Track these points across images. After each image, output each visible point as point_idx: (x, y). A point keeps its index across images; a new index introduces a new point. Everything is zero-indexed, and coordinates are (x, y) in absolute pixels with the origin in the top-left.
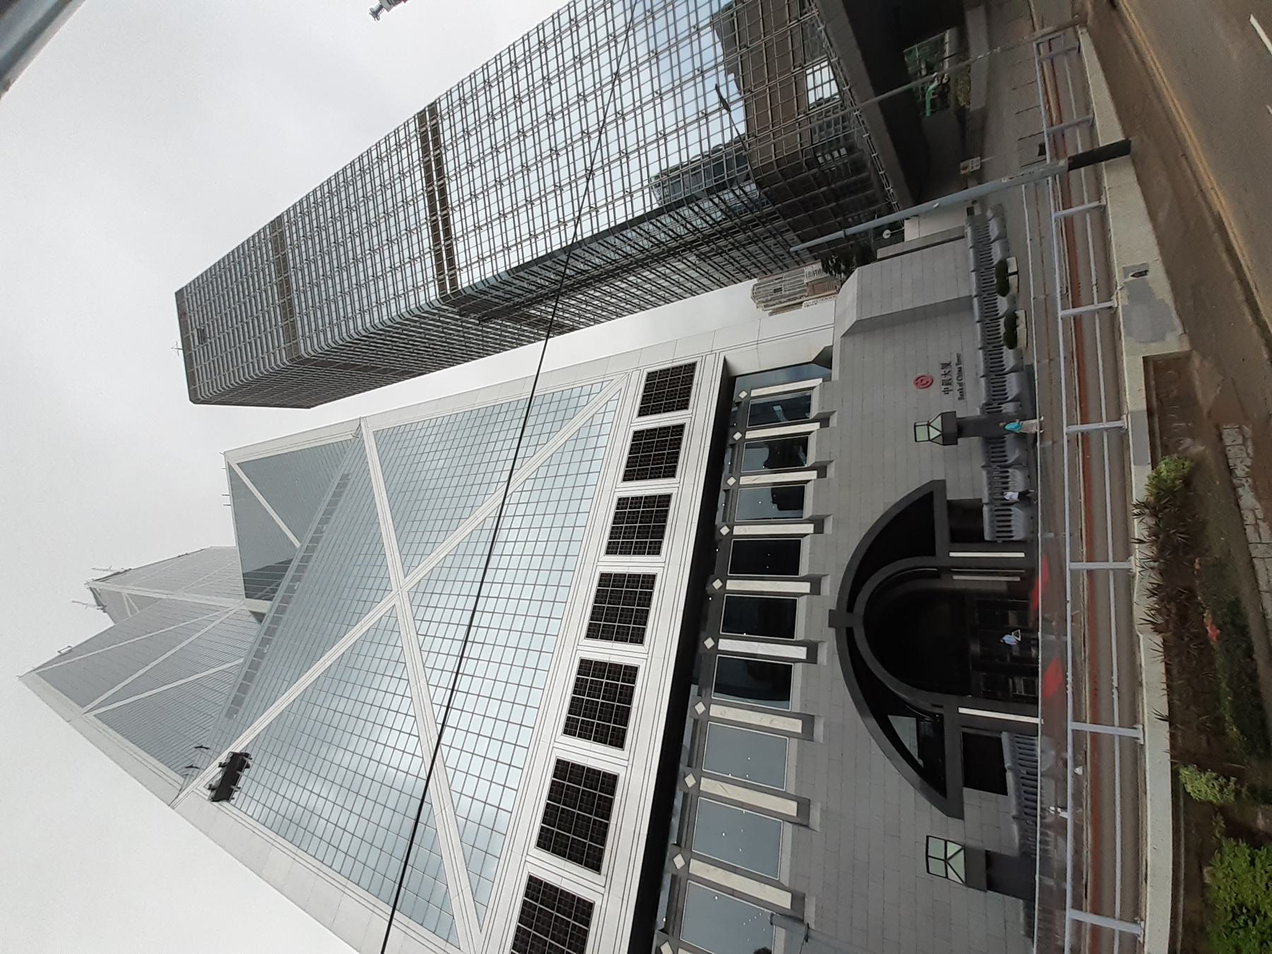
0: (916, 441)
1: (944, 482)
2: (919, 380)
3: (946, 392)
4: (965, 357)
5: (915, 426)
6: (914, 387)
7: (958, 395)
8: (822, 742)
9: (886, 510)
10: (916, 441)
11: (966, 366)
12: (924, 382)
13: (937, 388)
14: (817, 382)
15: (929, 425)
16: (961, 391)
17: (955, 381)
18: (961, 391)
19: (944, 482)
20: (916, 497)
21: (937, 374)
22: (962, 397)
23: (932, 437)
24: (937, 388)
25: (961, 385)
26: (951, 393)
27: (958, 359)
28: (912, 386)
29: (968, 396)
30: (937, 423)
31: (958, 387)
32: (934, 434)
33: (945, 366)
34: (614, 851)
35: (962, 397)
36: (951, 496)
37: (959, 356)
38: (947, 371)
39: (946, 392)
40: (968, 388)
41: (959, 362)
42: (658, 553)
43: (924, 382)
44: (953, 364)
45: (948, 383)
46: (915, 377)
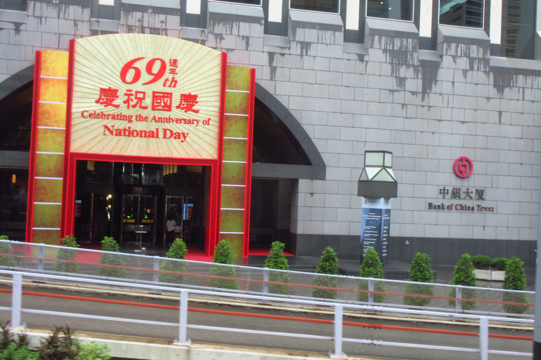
0: (366, 152)
1: (323, 178)
2: (466, 162)
3: (443, 192)
4: (489, 216)
5: (384, 152)
7: (436, 203)
9: (293, 113)
10: (366, 152)
11: (476, 217)
12: (463, 168)
13: (452, 182)
15: (384, 167)
16: (440, 207)
17: (455, 202)
18: (440, 207)
19: (323, 178)
20: (304, 145)
23: (367, 169)
24: (452, 182)
25: (450, 208)
26: (441, 196)
27: (486, 209)
28: (458, 154)
29: (433, 213)
30: (384, 177)
31: (447, 203)
32: (371, 173)
33: (480, 194)
35: (430, 205)
36: (303, 185)
37: (491, 209)
38: (473, 195)
39: (443, 192)
40: (442, 215)
41: (481, 209)
43: (463, 168)
44: (480, 202)
45: (456, 194)
46: (471, 158)
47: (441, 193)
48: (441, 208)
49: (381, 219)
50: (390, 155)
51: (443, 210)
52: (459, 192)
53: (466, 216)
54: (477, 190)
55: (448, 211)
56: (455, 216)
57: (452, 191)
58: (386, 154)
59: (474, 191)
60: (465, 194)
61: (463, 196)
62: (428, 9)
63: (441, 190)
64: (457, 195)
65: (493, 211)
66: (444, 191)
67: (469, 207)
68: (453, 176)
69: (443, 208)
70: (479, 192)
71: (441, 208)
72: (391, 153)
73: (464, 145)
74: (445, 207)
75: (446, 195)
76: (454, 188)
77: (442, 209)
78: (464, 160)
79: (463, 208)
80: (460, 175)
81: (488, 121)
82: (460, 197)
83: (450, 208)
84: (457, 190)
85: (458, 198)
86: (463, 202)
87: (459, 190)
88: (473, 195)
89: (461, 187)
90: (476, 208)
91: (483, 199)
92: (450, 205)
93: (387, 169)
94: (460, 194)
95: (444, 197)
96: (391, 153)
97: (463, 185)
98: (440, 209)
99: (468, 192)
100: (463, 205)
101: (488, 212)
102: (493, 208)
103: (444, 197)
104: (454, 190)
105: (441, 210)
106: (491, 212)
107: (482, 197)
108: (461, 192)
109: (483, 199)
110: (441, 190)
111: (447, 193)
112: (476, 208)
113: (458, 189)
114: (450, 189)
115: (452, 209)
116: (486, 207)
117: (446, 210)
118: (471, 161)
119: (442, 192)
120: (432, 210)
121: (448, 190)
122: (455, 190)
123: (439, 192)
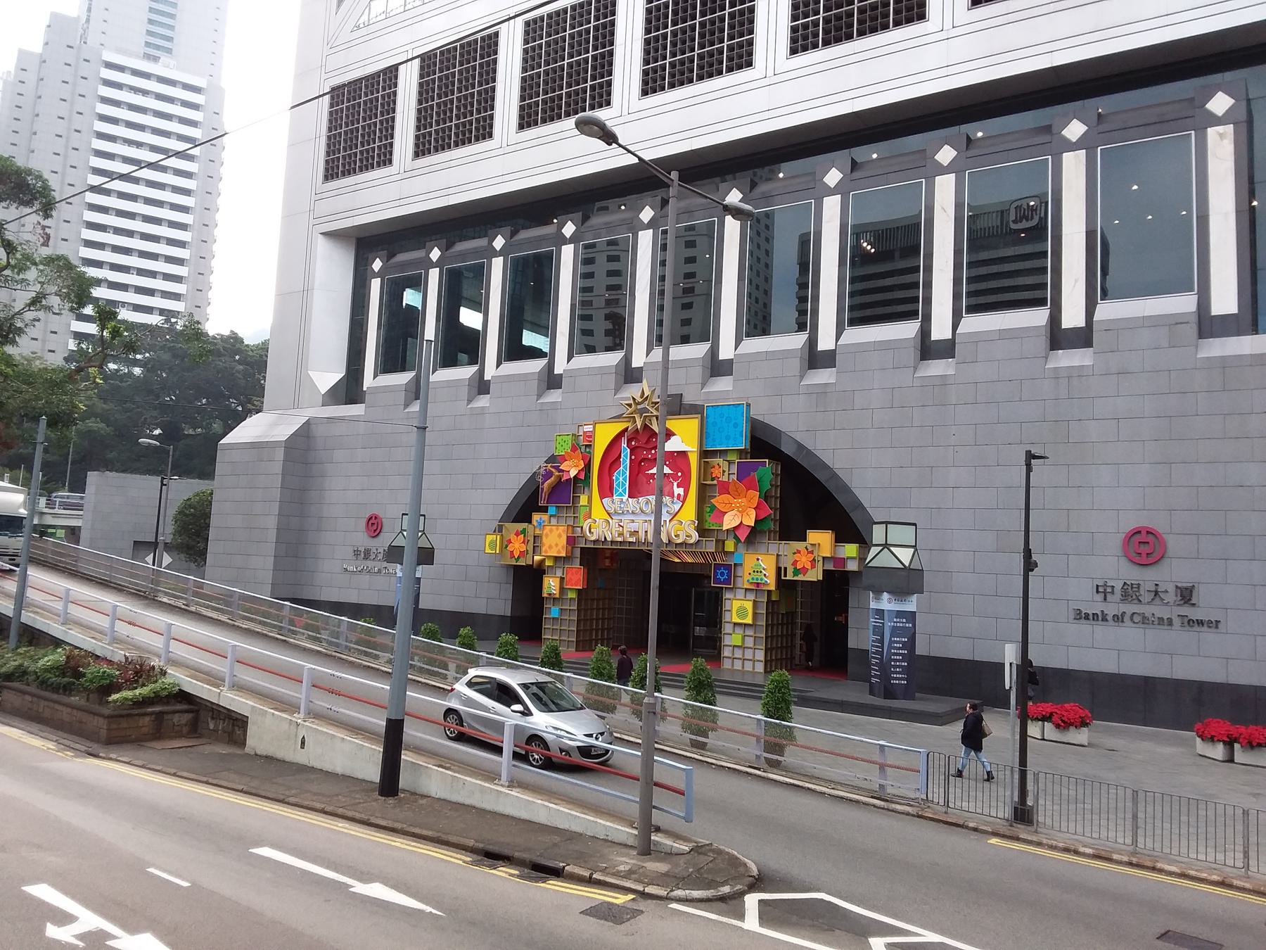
4: (1208, 635)
5: (887, 523)
6: (1133, 525)
8: (1198, 356)
9: (840, 473)
11: (1178, 637)
14: (1225, 300)
17: (1129, 608)
21: (1170, 574)
22: (1081, 616)
24: (1119, 571)
25: (1119, 619)
26: (1100, 597)
27: (1201, 623)
28: (1131, 522)
29: (1085, 627)
31: (1111, 609)
33: (1186, 595)
34: (432, 168)
39: (1103, 591)
40: (1101, 631)
42: (750, 64)
44: (1186, 611)
45: (1130, 592)
47: (1098, 592)
48: (1100, 619)
49: (883, 623)
50: (914, 527)
51: (1105, 623)
52: (1138, 591)
53: (1154, 636)
54: (1177, 587)
55: (1117, 624)
56: (1130, 634)
57: (1122, 588)
58: (888, 525)
59: (1171, 589)
60: (1153, 594)
61: (1146, 597)
62: (1076, 281)
63: (1097, 586)
64: (1134, 597)
65: (1217, 627)
66: (1105, 590)
67: (1161, 619)
68: (1124, 561)
69: (1104, 619)
70: (1181, 591)
71: (1100, 619)
72: (915, 524)
73: (1144, 506)
74: (1109, 618)
75: (1109, 596)
76: (1125, 583)
77: (1102, 620)
78: (1144, 533)
79: (1145, 620)
80: (1145, 560)
81: (1197, 460)
82: (1140, 601)
83: (1119, 619)
84: (1132, 588)
85: (1136, 601)
86: (1147, 610)
87: (1139, 588)
88: (1171, 597)
89: (1140, 582)
90: (1177, 621)
91: (1194, 605)
92: (1120, 614)
93: (892, 548)
94: (1141, 595)
95: (1105, 599)
96: (915, 524)
97: (1147, 577)
98: (1098, 620)
99: (1156, 593)
100: (1146, 615)
101: (1205, 628)
102: (1217, 622)
103: (1105, 599)
104: (1125, 587)
105: (1100, 623)
106: (1213, 630)
107: (1190, 600)
108: (1142, 592)
109: (1194, 605)
110: (1097, 586)
111: (1113, 593)
112: (1177, 621)
113: (1134, 586)
114: (1118, 586)
115: (1123, 621)
116: (1197, 620)
117: (1111, 623)
118: (1159, 534)
119: (1101, 589)
120: (1083, 621)
121: (1113, 587)
122: (1129, 588)
123: (1095, 590)
